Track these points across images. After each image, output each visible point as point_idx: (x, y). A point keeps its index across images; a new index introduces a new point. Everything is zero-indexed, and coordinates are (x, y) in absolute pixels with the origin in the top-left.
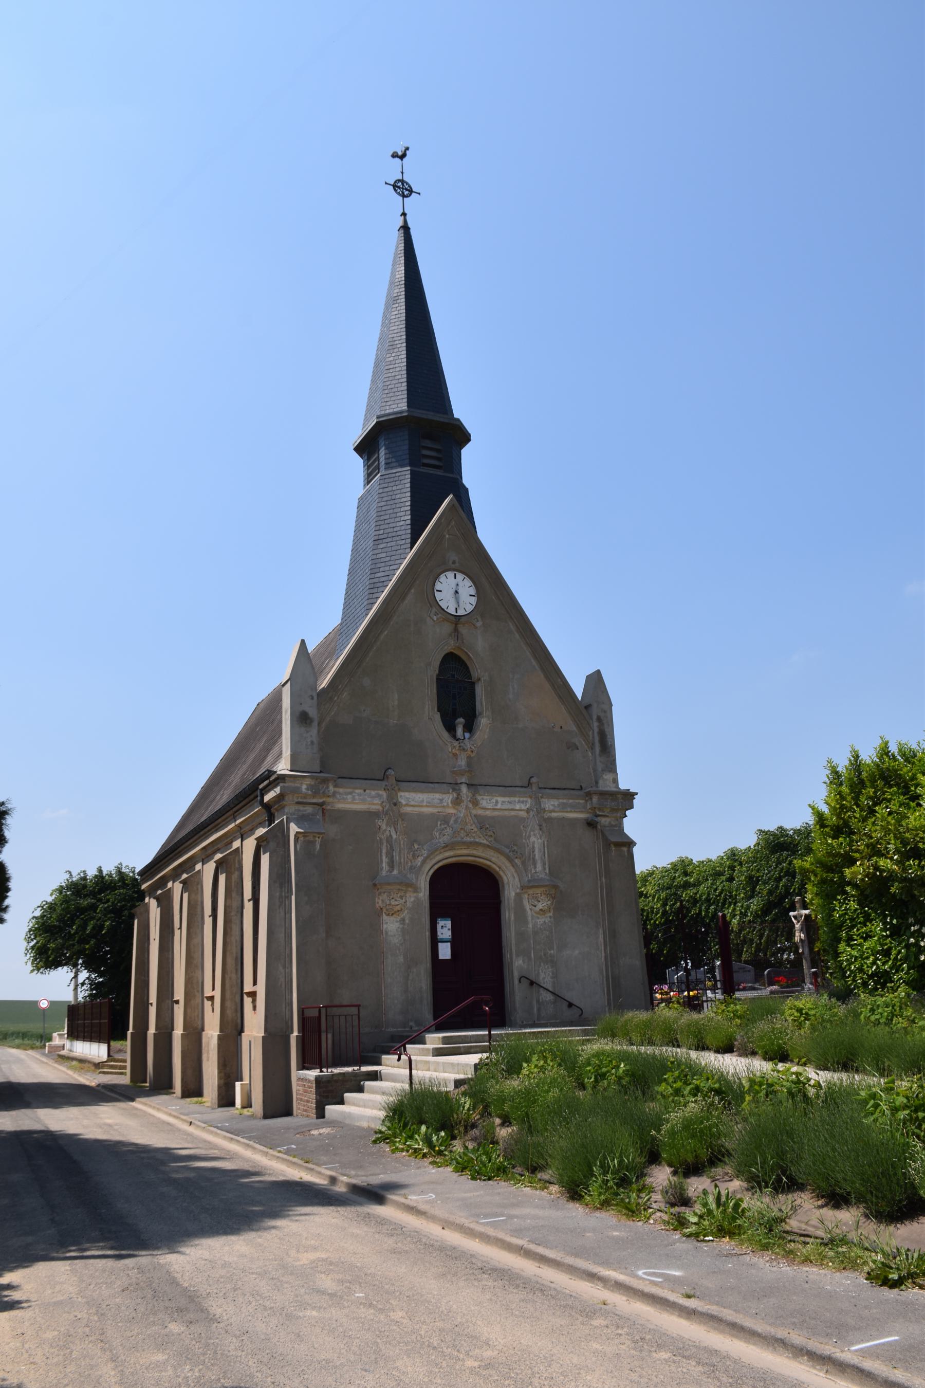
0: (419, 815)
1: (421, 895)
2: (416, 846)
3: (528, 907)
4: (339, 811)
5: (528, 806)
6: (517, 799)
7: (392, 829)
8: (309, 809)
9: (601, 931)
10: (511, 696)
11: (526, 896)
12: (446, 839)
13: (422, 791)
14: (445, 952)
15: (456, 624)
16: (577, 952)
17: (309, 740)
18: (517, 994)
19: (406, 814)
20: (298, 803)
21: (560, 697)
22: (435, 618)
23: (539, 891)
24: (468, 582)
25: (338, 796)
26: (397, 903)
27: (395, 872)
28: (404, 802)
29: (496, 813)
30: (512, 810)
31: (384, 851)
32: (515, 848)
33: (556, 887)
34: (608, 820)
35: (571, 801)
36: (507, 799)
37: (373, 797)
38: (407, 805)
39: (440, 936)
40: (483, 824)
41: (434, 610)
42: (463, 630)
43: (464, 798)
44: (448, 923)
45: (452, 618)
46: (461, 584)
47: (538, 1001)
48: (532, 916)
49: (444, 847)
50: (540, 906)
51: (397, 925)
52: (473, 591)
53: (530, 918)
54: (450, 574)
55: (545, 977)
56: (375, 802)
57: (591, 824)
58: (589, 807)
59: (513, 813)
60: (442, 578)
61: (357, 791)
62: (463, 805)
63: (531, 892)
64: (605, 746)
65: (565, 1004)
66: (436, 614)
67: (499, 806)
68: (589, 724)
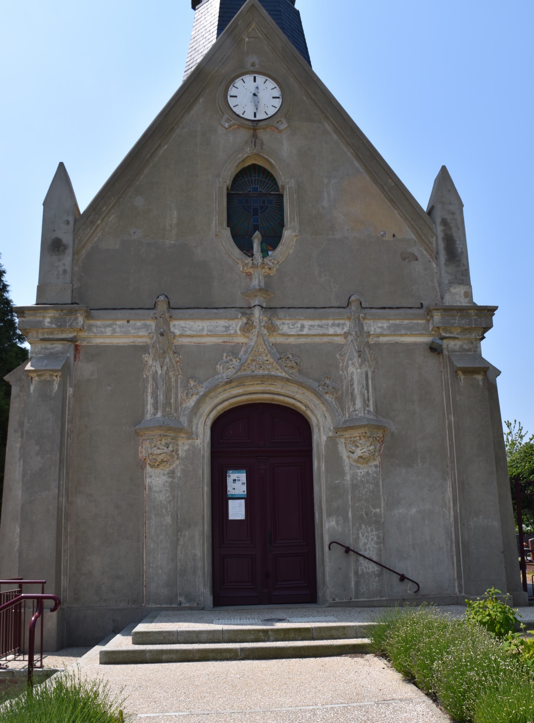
0: (200, 347)
1: (198, 442)
2: (192, 383)
3: (344, 454)
4: (97, 347)
5: (346, 330)
6: (330, 322)
7: (158, 365)
8: (58, 347)
9: (449, 483)
10: (325, 203)
11: (343, 440)
12: (230, 373)
13: (202, 319)
14: (237, 511)
15: (255, 130)
16: (414, 510)
17: (61, 270)
18: (328, 563)
19: (182, 346)
20: (43, 340)
21: (392, 201)
22: (227, 125)
23: (356, 433)
24: (271, 84)
25: (95, 330)
26: (159, 451)
27: (159, 415)
28: (177, 332)
29: (302, 340)
30: (324, 335)
31: (150, 390)
32: (328, 382)
33: (383, 428)
34: (458, 343)
35: (406, 322)
36: (317, 322)
37: (139, 329)
38: (181, 336)
39: (231, 491)
40: (282, 353)
41: (226, 116)
42: (263, 135)
43: (256, 323)
44: (242, 476)
45: (250, 123)
46: (262, 86)
47: (356, 573)
48: (351, 465)
49: (227, 383)
50: (359, 452)
51: (165, 478)
52: (277, 92)
53: (347, 468)
54: (249, 79)
55: (367, 542)
56: (141, 334)
57: (434, 349)
58: (431, 327)
59: (325, 339)
60: (238, 83)
61: (119, 323)
62: (255, 331)
63: (347, 434)
64: (455, 254)
65: (396, 578)
66: (228, 120)
67: (305, 331)
68: (430, 229)
